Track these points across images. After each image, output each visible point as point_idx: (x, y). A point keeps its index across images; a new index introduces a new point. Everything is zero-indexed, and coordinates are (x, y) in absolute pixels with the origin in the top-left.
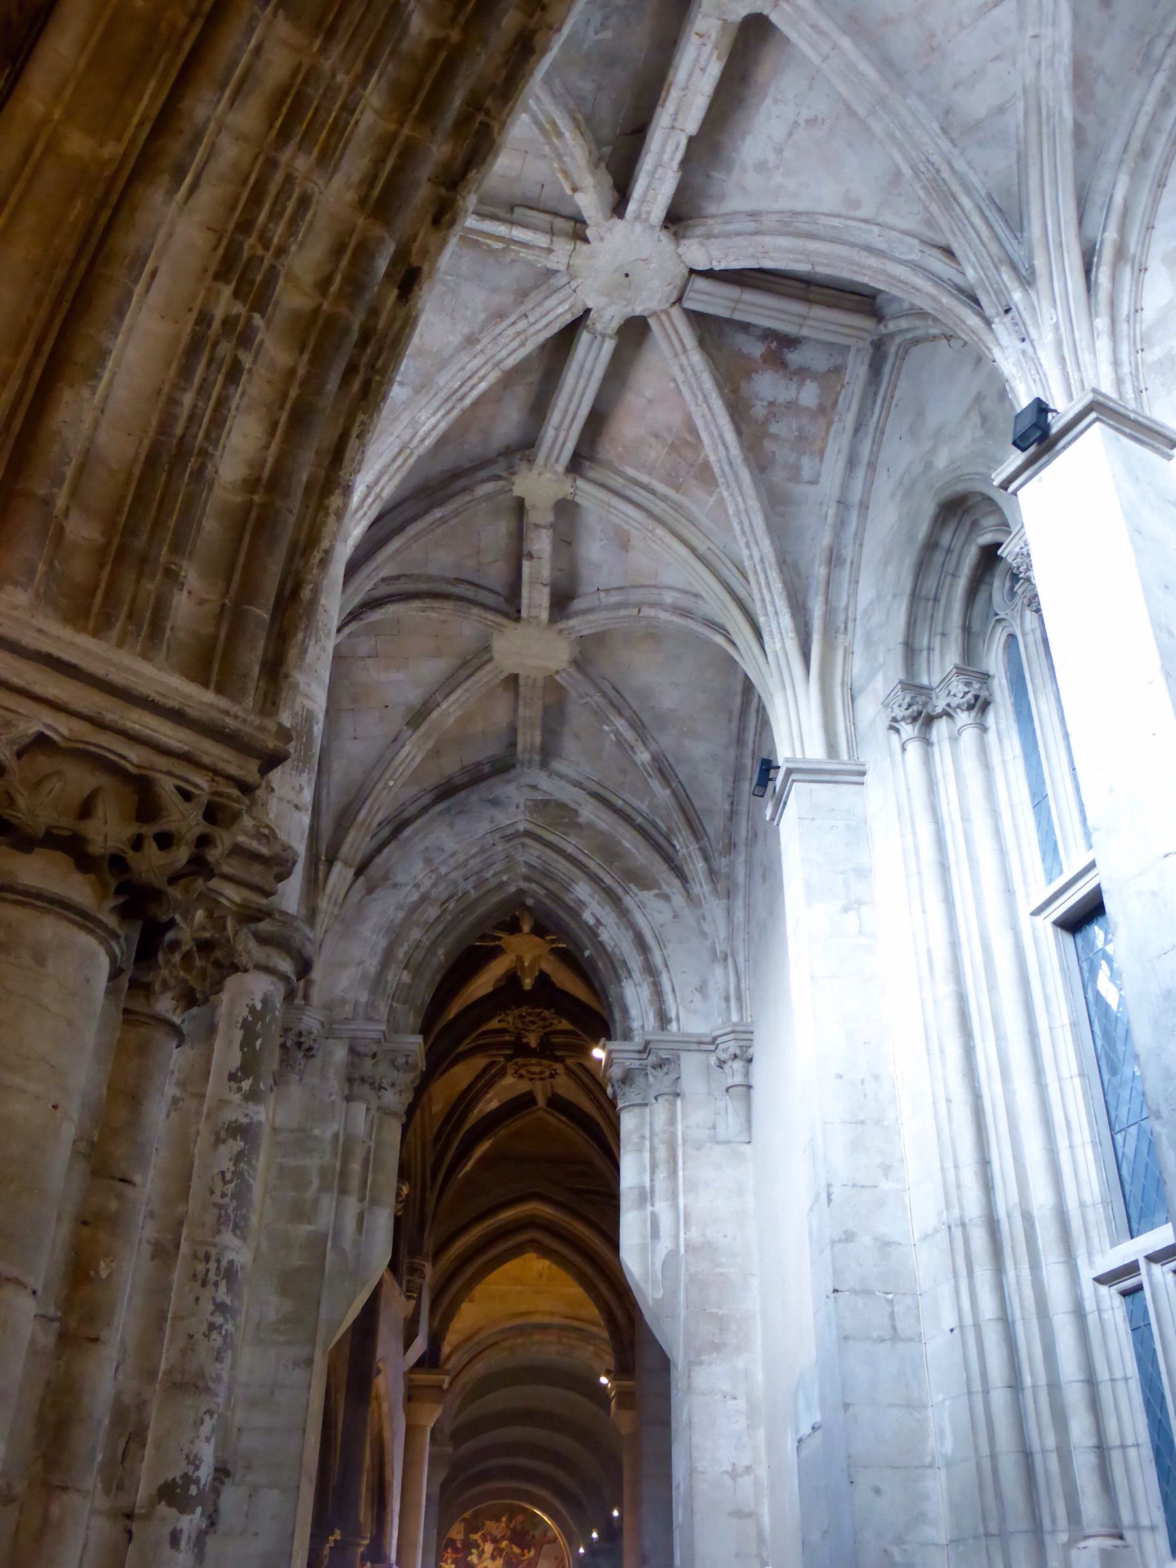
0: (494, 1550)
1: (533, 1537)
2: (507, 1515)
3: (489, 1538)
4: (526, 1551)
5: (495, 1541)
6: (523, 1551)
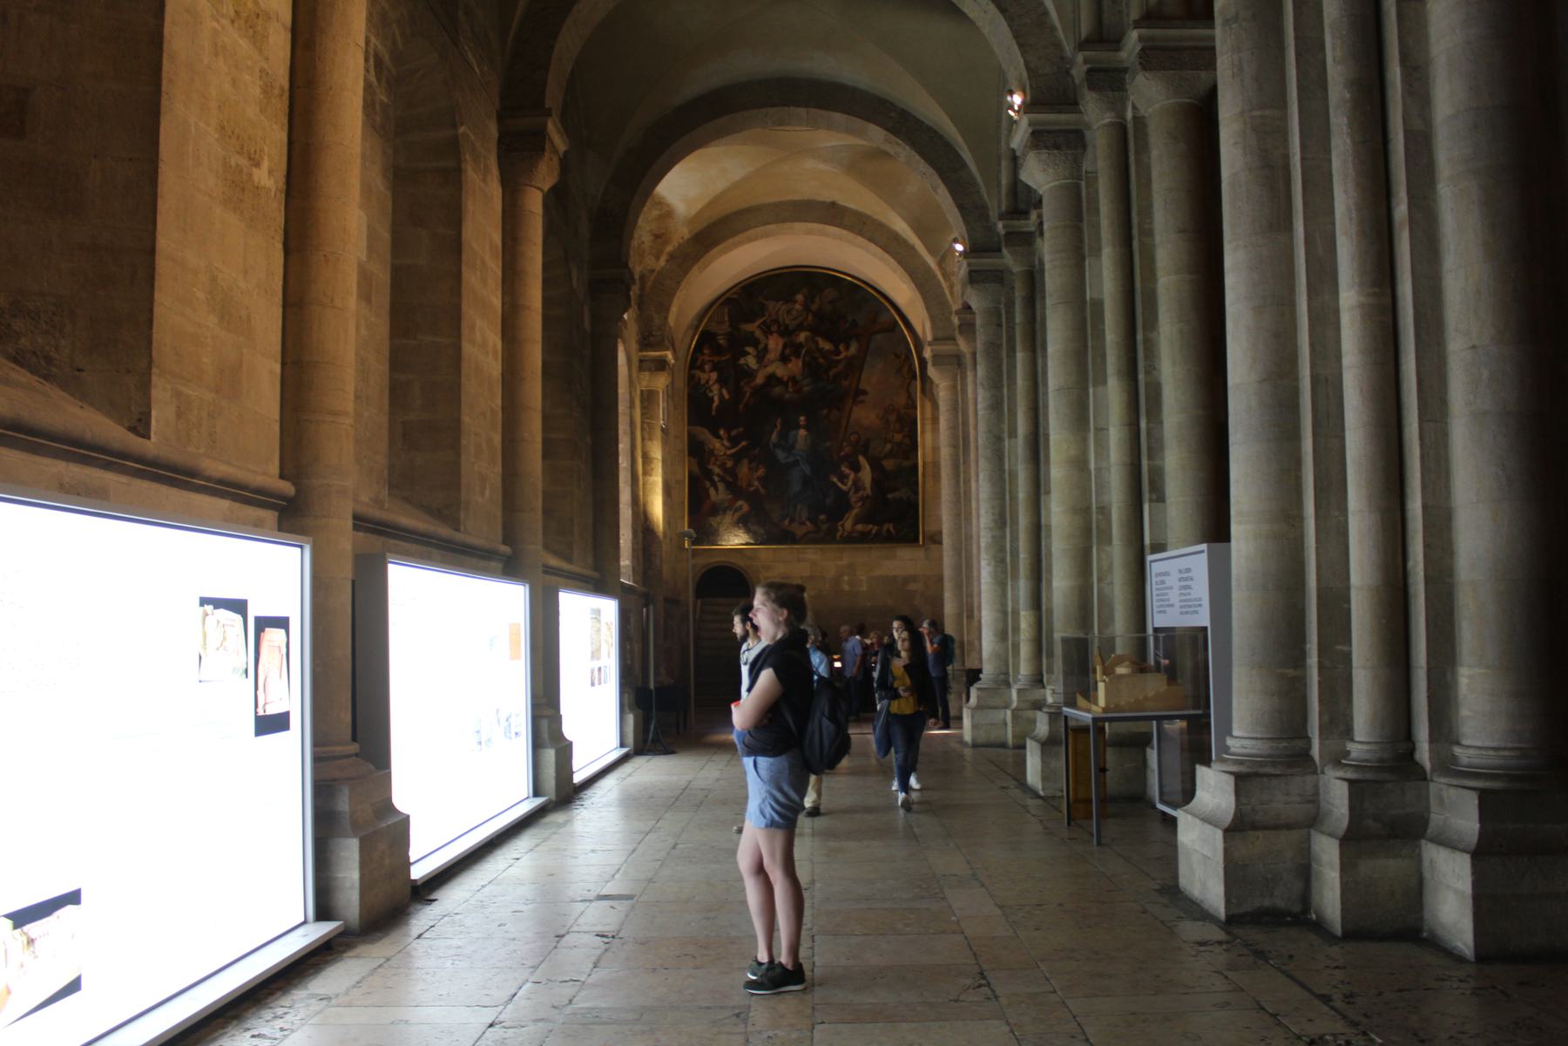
0: (785, 347)
3: (774, 328)
4: (841, 347)
5: (785, 332)
6: (837, 347)
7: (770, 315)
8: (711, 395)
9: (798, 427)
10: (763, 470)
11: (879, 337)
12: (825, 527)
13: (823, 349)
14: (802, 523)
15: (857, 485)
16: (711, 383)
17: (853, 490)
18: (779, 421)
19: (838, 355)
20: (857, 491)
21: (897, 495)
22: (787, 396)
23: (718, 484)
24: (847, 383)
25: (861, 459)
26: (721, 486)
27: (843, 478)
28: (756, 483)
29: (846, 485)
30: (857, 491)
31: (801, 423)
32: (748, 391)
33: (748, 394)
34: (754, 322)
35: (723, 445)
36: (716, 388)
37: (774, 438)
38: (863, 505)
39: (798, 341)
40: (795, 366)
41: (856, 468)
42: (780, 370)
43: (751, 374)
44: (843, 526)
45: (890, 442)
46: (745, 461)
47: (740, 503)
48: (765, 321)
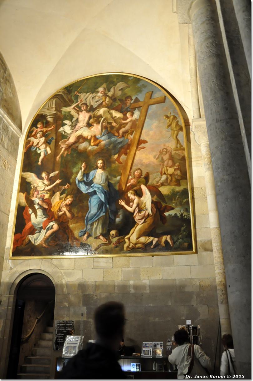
0: (90, 118)
1: (137, 100)
2: (105, 85)
3: (83, 108)
4: (128, 115)
5: (91, 109)
6: (125, 115)
7: (81, 101)
8: (39, 152)
9: (97, 168)
10: (70, 199)
11: (154, 107)
12: (115, 240)
13: (116, 117)
14: (98, 238)
15: (140, 208)
16: (40, 144)
17: (137, 210)
18: (83, 165)
19: (126, 120)
20: (140, 211)
21: (172, 213)
22: (90, 148)
23: (38, 210)
24: (132, 137)
25: (143, 187)
26: (40, 212)
27: (129, 202)
28: (64, 209)
29: (132, 207)
30: (140, 211)
31: (99, 165)
32: (63, 147)
33: (63, 149)
34: (71, 106)
35: (44, 183)
36: (43, 147)
37: (79, 177)
38: (144, 222)
39: (99, 114)
40: (97, 129)
41: (139, 194)
42: (86, 133)
43: (65, 137)
44: (129, 239)
45: (165, 173)
46: (58, 194)
47: (51, 224)
48: (78, 104)
